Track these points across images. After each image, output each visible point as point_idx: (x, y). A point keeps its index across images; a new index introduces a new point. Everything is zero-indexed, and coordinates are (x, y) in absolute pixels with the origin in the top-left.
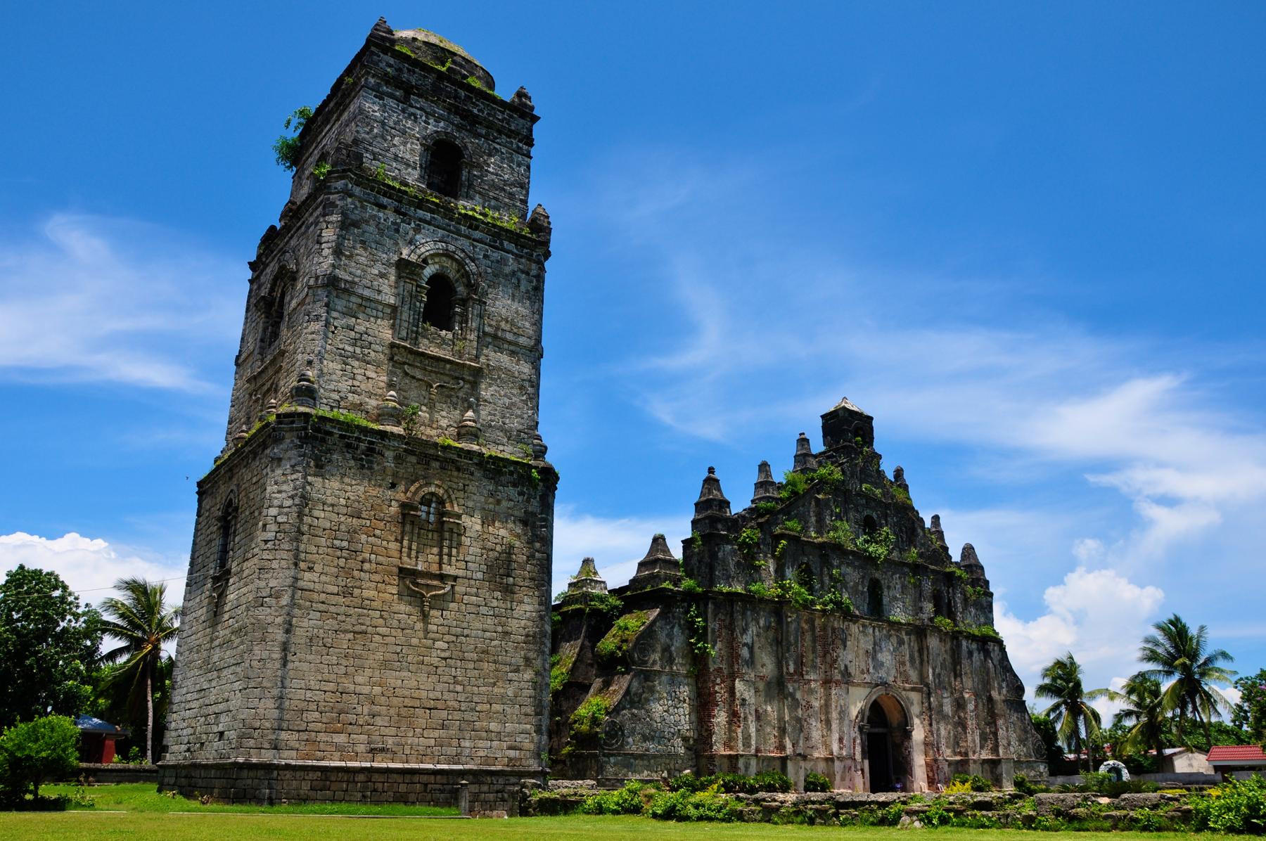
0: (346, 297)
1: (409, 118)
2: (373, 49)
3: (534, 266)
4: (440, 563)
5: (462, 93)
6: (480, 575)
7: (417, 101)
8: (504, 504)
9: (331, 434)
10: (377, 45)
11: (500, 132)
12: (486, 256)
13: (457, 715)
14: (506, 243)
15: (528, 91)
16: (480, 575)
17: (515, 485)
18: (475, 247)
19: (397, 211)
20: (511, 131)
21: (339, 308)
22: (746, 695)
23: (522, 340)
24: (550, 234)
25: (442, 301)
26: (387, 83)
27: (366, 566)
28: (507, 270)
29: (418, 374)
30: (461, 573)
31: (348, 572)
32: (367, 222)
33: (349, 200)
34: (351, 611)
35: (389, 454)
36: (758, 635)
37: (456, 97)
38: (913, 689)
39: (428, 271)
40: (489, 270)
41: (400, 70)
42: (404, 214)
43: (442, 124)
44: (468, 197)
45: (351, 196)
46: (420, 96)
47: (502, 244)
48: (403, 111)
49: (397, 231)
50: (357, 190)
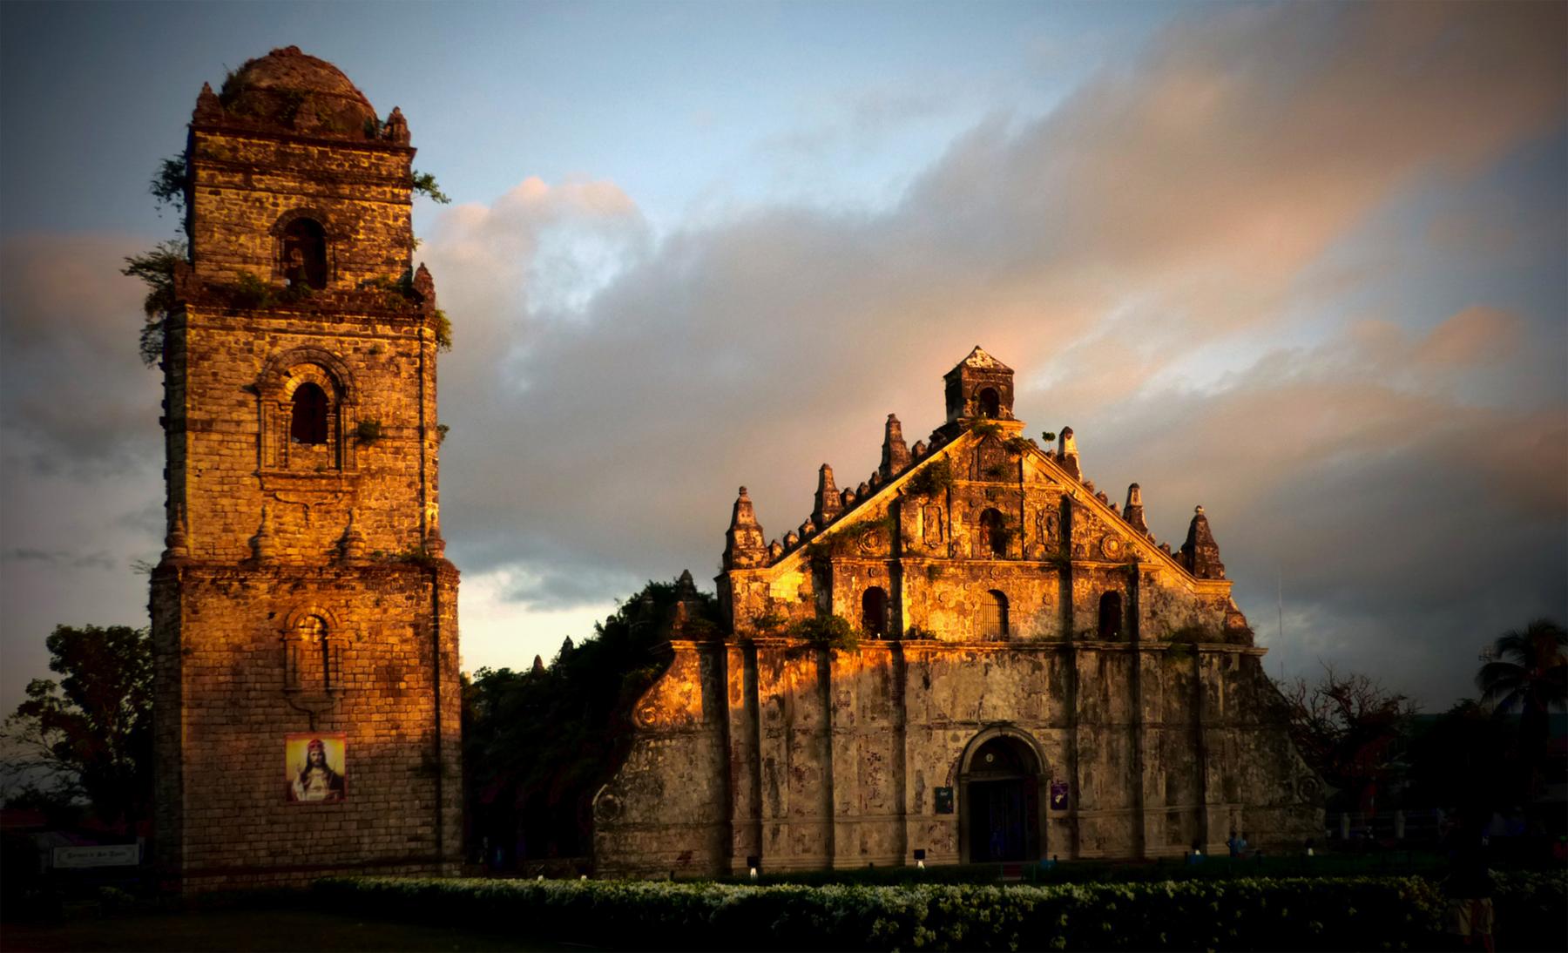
0: (205, 436)
1: (253, 206)
2: (199, 134)
3: (416, 344)
4: (327, 679)
5: (315, 150)
6: (369, 685)
7: (260, 181)
8: (392, 611)
9: (203, 580)
10: (203, 129)
11: (368, 185)
12: (356, 350)
13: (354, 816)
14: (379, 327)
15: (405, 113)
16: (369, 685)
17: (401, 590)
18: (342, 342)
19: (247, 329)
21: (200, 450)
24: (433, 300)
25: (313, 416)
26: (221, 171)
27: (253, 694)
28: (383, 358)
29: (292, 498)
30: (350, 685)
32: (216, 350)
33: (193, 332)
34: (243, 736)
35: (264, 587)
37: (308, 156)
38: (1052, 726)
39: (292, 385)
40: (362, 365)
41: (234, 150)
42: (256, 330)
43: (294, 200)
44: (336, 278)
45: (193, 327)
46: (262, 173)
47: (374, 329)
48: (246, 200)
49: (250, 351)
50: (201, 319)
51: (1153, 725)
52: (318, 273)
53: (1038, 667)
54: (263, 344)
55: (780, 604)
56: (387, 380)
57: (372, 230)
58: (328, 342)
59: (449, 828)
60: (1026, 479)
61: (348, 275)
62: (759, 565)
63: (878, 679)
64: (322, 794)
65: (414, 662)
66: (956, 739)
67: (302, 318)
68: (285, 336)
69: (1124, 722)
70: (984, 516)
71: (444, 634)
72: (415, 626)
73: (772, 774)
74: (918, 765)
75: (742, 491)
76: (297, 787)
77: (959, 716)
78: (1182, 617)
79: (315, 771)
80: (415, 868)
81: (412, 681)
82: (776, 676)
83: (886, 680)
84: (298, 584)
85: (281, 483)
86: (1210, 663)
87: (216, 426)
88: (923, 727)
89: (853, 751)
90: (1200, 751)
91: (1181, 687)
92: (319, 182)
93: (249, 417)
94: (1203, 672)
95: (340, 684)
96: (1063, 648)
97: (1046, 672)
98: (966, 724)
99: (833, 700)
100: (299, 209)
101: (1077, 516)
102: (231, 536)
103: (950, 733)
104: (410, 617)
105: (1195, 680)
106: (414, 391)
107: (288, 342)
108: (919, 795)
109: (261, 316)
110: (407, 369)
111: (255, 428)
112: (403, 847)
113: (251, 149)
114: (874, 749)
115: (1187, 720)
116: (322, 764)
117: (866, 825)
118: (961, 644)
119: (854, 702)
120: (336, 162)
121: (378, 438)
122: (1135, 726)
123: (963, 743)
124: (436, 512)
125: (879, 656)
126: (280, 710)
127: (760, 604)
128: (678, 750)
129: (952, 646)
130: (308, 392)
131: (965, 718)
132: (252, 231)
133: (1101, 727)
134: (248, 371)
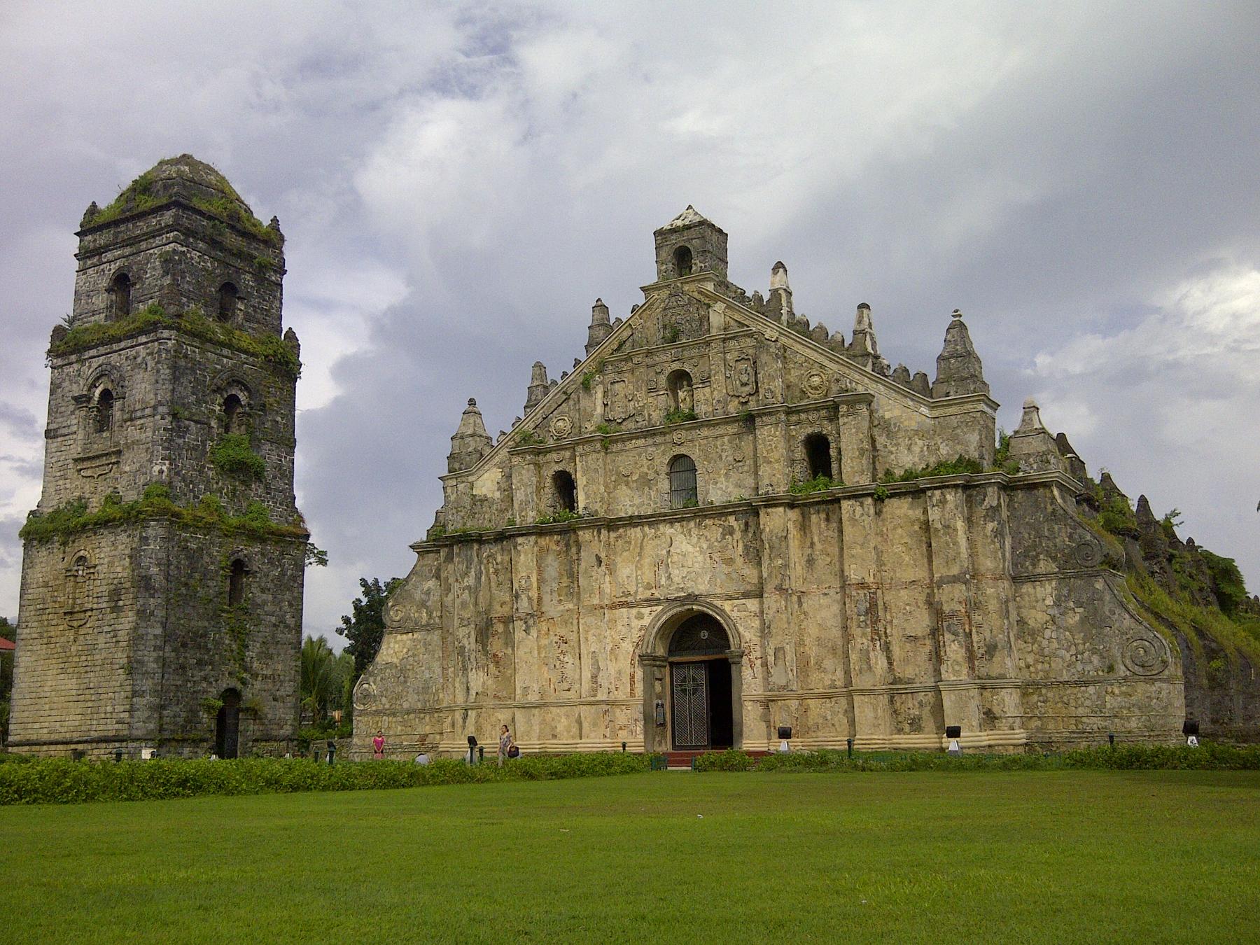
5: (131, 226)
11: (154, 237)
16: (104, 605)
20: (162, 229)
22: (465, 642)
23: (147, 411)
29: (89, 473)
30: (95, 606)
36: (496, 572)
39: (97, 392)
41: (95, 240)
50: (59, 362)
53: (731, 534)
57: (154, 269)
65: (128, 585)
66: (640, 616)
71: (146, 562)
72: (130, 557)
86: (943, 502)
87: (60, 432)
92: (131, 245)
94: (934, 515)
95: (90, 606)
96: (750, 510)
97: (738, 535)
98: (651, 602)
99: (516, 586)
100: (120, 268)
103: (634, 611)
104: (128, 551)
105: (926, 526)
107: (96, 363)
108: (594, 678)
110: (151, 364)
111: (74, 428)
113: (102, 239)
118: (639, 517)
120: (141, 227)
123: (647, 621)
126: (61, 628)
129: (633, 521)
130: (106, 394)
131: (648, 594)
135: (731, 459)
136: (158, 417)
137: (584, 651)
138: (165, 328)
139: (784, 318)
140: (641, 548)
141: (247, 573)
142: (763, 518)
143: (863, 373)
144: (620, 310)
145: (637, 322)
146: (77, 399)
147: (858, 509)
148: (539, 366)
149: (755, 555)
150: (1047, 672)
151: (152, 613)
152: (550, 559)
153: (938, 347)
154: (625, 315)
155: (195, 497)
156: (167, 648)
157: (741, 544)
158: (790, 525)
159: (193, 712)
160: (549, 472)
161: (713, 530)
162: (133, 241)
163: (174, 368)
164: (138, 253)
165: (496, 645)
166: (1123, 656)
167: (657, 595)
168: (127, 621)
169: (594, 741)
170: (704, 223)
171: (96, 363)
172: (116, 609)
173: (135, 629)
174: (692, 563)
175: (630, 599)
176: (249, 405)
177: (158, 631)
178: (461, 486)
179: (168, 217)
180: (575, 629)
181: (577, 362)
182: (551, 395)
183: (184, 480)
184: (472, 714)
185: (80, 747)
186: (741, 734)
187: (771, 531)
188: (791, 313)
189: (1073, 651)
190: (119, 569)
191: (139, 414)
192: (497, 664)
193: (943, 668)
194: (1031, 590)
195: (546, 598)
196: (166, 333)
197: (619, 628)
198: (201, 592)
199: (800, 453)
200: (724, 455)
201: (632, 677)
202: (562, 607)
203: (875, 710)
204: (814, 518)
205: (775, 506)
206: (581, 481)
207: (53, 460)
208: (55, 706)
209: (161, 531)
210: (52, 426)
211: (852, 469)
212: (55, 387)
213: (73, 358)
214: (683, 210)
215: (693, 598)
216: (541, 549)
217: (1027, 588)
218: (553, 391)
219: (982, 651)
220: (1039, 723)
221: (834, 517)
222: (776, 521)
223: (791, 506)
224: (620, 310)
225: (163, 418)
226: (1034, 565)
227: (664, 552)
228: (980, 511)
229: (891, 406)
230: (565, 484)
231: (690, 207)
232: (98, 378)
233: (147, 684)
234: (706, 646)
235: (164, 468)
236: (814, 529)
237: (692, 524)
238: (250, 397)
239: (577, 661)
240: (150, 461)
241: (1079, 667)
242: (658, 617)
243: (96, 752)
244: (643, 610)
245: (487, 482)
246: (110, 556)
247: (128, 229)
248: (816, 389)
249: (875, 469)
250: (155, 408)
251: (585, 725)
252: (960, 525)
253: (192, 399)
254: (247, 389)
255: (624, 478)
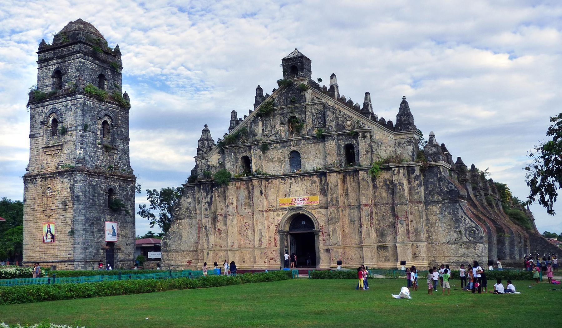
8: (66, 184)
11: (71, 55)
16: (60, 207)
17: (67, 177)
19: (42, 106)
20: (74, 52)
30: (56, 208)
31: (34, 215)
35: (40, 180)
36: (219, 196)
38: (321, 208)
39: (51, 119)
50: (33, 106)
51: (367, 205)
52: (60, 85)
53: (315, 182)
54: (45, 110)
55: (212, 167)
56: (69, 114)
57: (72, 69)
58: (57, 106)
59: (78, 251)
60: (307, 101)
61: (67, 84)
62: (205, 153)
63: (246, 193)
64: (50, 240)
65: (70, 199)
67: (52, 100)
68: (49, 106)
69: (357, 204)
70: (289, 121)
71: (76, 190)
72: (70, 188)
73: (206, 232)
74: (260, 227)
75: (206, 126)
76: (45, 238)
77: (279, 206)
78: (388, 151)
79: (49, 233)
80: (69, 263)
81: (69, 205)
82: (207, 194)
83: (249, 193)
84: (46, 179)
85: (48, 149)
86: (399, 173)
87: (36, 135)
88: (260, 211)
89: (235, 221)
90: (395, 216)
91: (387, 185)
93: (41, 131)
94: (395, 178)
95: (54, 208)
96: (322, 174)
97: (318, 184)
101: (328, 113)
102: (38, 166)
103: (276, 213)
104: (69, 186)
105: (392, 182)
106: (75, 115)
107: (50, 107)
108: (260, 239)
109: (44, 102)
110: (73, 109)
111: (42, 134)
112: (66, 257)
114: (246, 221)
115: (390, 201)
116: (50, 232)
117: (244, 251)
118: (277, 176)
119: (235, 203)
121: (67, 132)
122: (359, 207)
123: (281, 217)
124: (81, 152)
125: (246, 183)
127: (205, 168)
128: (187, 223)
129: (275, 177)
130: (55, 121)
131: (282, 206)
132: (47, 77)
133: (345, 207)
134: (41, 118)
135: (314, 153)
136: (78, 131)
137: (256, 229)
138: (79, 94)
139: (336, 96)
140: (279, 187)
141: (115, 193)
142: (328, 178)
143: (368, 121)
144: (268, 90)
145: (275, 96)
146: (43, 123)
147: (366, 175)
148: (234, 112)
149: (324, 192)
150: (437, 239)
151: (80, 211)
152: (242, 190)
153: (397, 111)
154: (270, 93)
155: (94, 163)
156: (87, 225)
157: (319, 187)
158: (339, 180)
159: (98, 250)
160: (240, 156)
161: (308, 181)
162: (62, 57)
163: (83, 110)
164: (64, 62)
165: (220, 226)
166: (465, 233)
167: (285, 206)
168: (70, 214)
169: (262, 264)
170: (302, 56)
171: (50, 107)
172: (65, 209)
173: (74, 217)
174: (300, 195)
175: (274, 208)
176: (111, 124)
177: (83, 218)
178: (203, 161)
179: (77, 47)
180: (252, 219)
181: (250, 112)
182: (240, 124)
183: (89, 156)
184: (211, 253)
185: (54, 264)
186: (319, 262)
187: (331, 183)
188: (339, 95)
189: (447, 231)
190: (65, 193)
191: (70, 129)
192: (220, 233)
193: (397, 237)
194: (431, 208)
195: (240, 207)
196: (79, 96)
197: (270, 220)
198: (97, 202)
199: (342, 151)
200: (312, 151)
201: (275, 239)
202: (246, 211)
203: (371, 252)
204: (348, 177)
205: (333, 172)
206: (253, 160)
207: (33, 147)
208: (41, 247)
209: (82, 178)
210: (32, 133)
211: (364, 160)
212: (32, 117)
213: (39, 105)
214: (293, 50)
215: (299, 208)
216: (237, 188)
217: (430, 207)
218: (241, 123)
219: (413, 231)
220: (433, 259)
221: (356, 178)
222: (333, 179)
223: (339, 173)
224: (268, 90)
225: (80, 131)
226: (433, 198)
227: (288, 190)
228: (412, 176)
229: (379, 134)
230: (247, 161)
231: (296, 49)
232: (51, 114)
233: (79, 239)
234: (305, 227)
235: (81, 152)
236: (348, 182)
237: (299, 179)
238: (112, 121)
239: (253, 233)
240: (75, 149)
241: (449, 238)
242: (286, 216)
243: (60, 266)
244: (279, 213)
245: (214, 159)
246: (61, 187)
247: (59, 52)
248: (349, 126)
249: (372, 159)
250: (76, 127)
251: (257, 258)
252: (405, 182)
253: (91, 123)
254: (111, 118)
255: (271, 160)
